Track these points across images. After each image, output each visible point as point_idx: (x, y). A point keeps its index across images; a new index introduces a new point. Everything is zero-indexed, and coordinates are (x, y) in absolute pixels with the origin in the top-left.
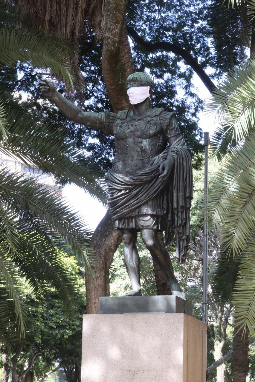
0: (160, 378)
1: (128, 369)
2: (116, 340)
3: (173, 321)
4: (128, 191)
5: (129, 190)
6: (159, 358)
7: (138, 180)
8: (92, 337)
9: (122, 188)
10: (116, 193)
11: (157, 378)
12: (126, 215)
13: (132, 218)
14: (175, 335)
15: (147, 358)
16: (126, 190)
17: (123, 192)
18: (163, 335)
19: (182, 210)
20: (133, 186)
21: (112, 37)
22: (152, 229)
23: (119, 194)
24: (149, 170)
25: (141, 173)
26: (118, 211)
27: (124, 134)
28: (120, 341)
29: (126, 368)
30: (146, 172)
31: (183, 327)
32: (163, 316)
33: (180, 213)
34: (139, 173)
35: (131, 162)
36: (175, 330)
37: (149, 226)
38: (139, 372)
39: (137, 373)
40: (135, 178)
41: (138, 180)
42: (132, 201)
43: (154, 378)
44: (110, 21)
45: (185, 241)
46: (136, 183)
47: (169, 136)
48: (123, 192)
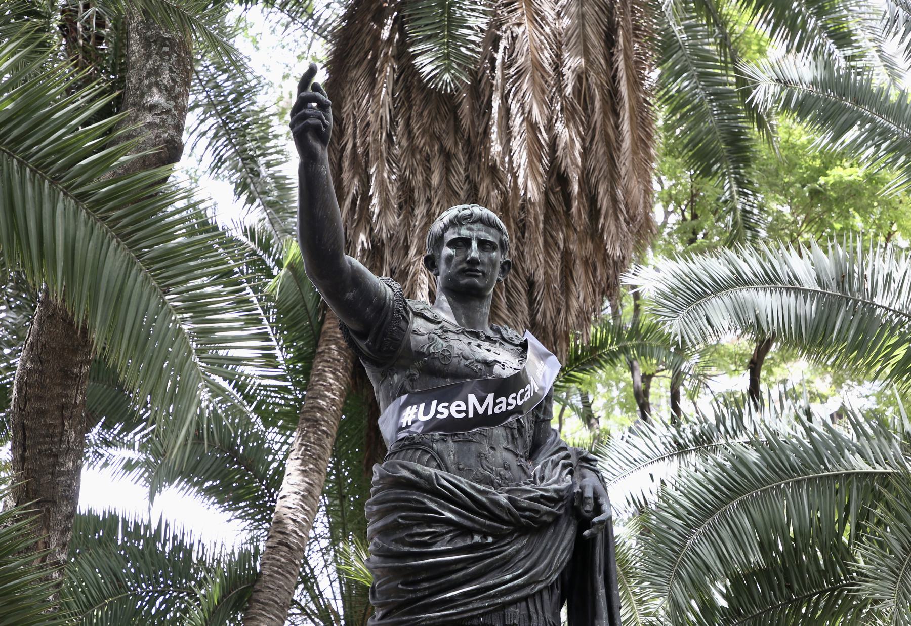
4: (490, 540)
5: (493, 537)
7: (527, 513)
9: (476, 526)
10: (448, 537)
12: (472, 618)
16: (485, 537)
17: (477, 539)
20: (511, 528)
21: (176, 113)
23: (460, 543)
24: (556, 491)
25: (541, 493)
26: (452, 599)
27: (467, 363)
30: (549, 495)
34: (529, 492)
35: (492, 452)
40: (525, 504)
41: (527, 513)
42: (508, 577)
44: (171, 70)
46: (523, 520)
47: (542, 417)
48: (477, 539)
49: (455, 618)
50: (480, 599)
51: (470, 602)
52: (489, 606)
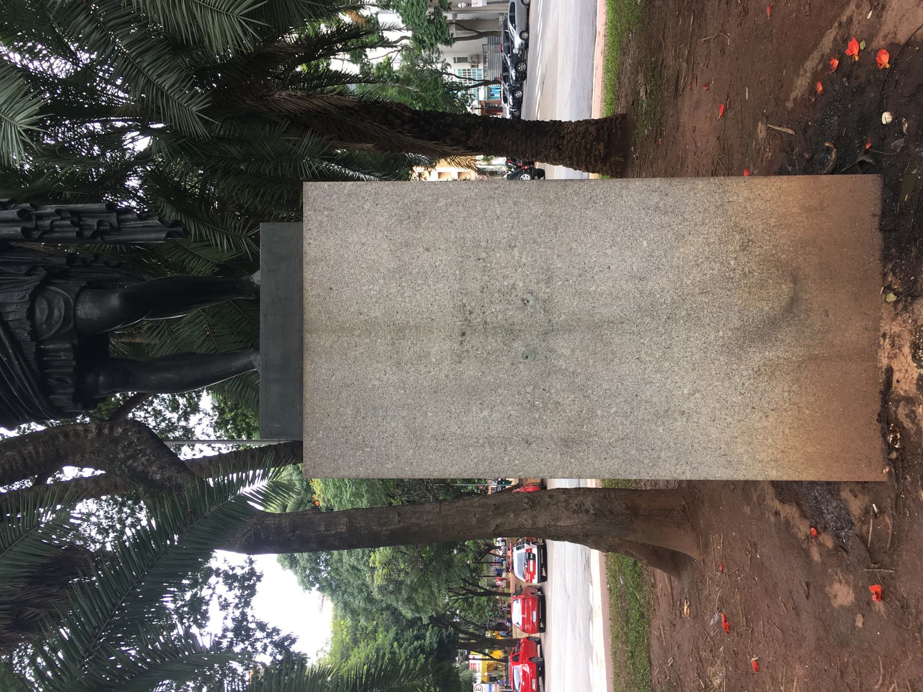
0: (483, 244)
1: (460, 338)
2: (378, 376)
3: (326, 213)
6: (428, 250)
8: (369, 449)
11: (484, 255)
13: (40, 353)
14: (365, 206)
15: (429, 286)
18: (364, 240)
19: (34, 217)
22: (78, 296)
26: (19, 391)
28: (379, 365)
29: (456, 346)
31: (344, 183)
32: (311, 241)
33: (41, 223)
36: (351, 206)
37: (67, 302)
38: (468, 308)
39: (471, 313)
43: (481, 264)
45: (123, 217)
49: (35, 386)
50: (12, 369)
51: (18, 375)
52: (18, 360)
